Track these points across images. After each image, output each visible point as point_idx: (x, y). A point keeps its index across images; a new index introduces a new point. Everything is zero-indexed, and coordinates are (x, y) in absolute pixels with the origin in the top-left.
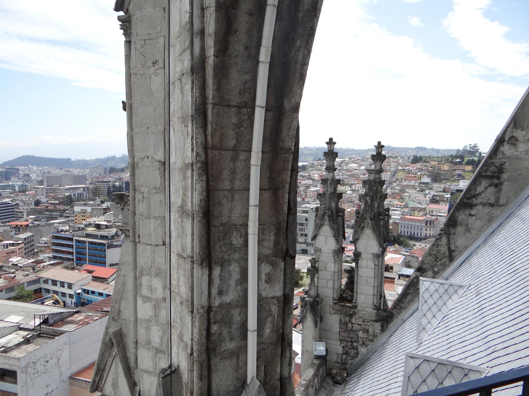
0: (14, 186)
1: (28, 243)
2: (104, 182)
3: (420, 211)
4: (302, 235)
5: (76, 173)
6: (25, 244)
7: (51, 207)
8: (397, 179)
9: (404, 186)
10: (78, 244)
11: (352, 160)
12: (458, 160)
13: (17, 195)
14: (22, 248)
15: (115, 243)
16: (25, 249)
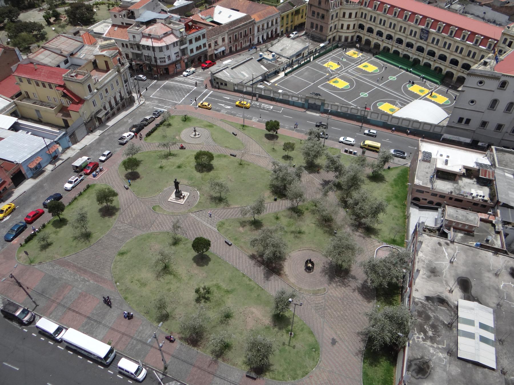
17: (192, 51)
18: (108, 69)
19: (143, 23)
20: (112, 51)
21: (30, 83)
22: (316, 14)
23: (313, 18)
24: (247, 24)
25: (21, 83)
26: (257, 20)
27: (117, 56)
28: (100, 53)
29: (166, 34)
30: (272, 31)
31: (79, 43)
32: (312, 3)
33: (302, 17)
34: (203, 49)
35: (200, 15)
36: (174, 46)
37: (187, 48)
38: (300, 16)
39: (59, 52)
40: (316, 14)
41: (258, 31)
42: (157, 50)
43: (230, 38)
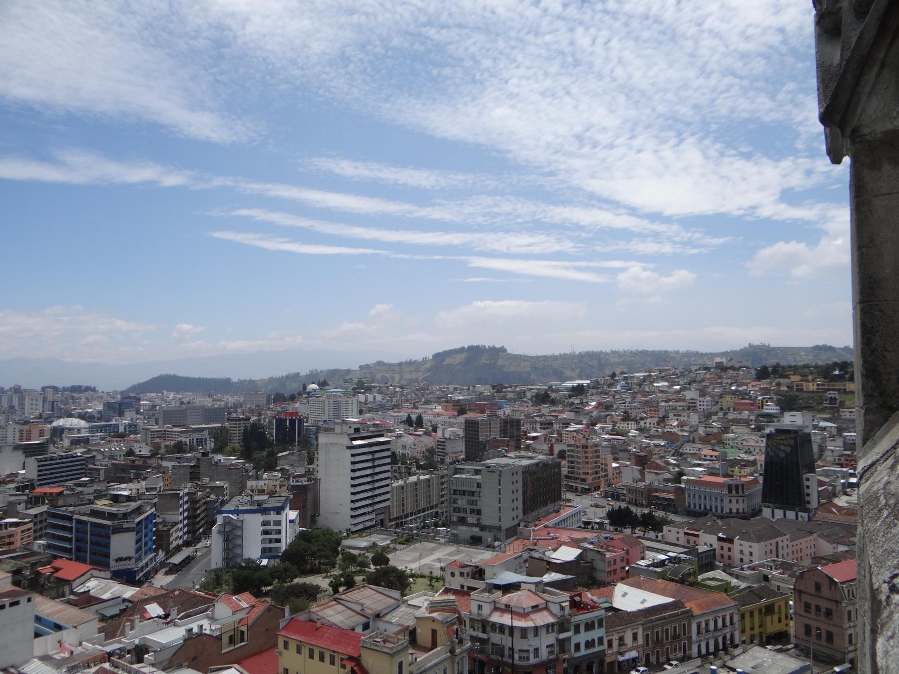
0: (117, 426)
1: (41, 522)
2: (240, 420)
3: (745, 466)
4: (472, 511)
5: (210, 405)
6: (35, 524)
7: (139, 463)
8: (721, 409)
9: (729, 421)
10: (80, 526)
11: (663, 374)
12: (837, 372)
13: (110, 441)
14: (29, 530)
15: (125, 526)
16: (35, 531)
17: (577, 646)
18: (434, 645)
19: (497, 587)
20: (447, 614)
21: (299, 651)
22: (813, 607)
23: (808, 615)
24: (677, 615)
25: (284, 651)
26: (696, 612)
27: (454, 624)
28: (427, 615)
29: (536, 608)
30: (724, 638)
31: (392, 601)
32: (802, 588)
33: (780, 621)
34: (597, 648)
35: (589, 595)
36: (548, 632)
37: (569, 639)
38: (776, 617)
39: (358, 608)
40: (813, 607)
41: (699, 633)
42: (517, 634)
43: (647, 635)
